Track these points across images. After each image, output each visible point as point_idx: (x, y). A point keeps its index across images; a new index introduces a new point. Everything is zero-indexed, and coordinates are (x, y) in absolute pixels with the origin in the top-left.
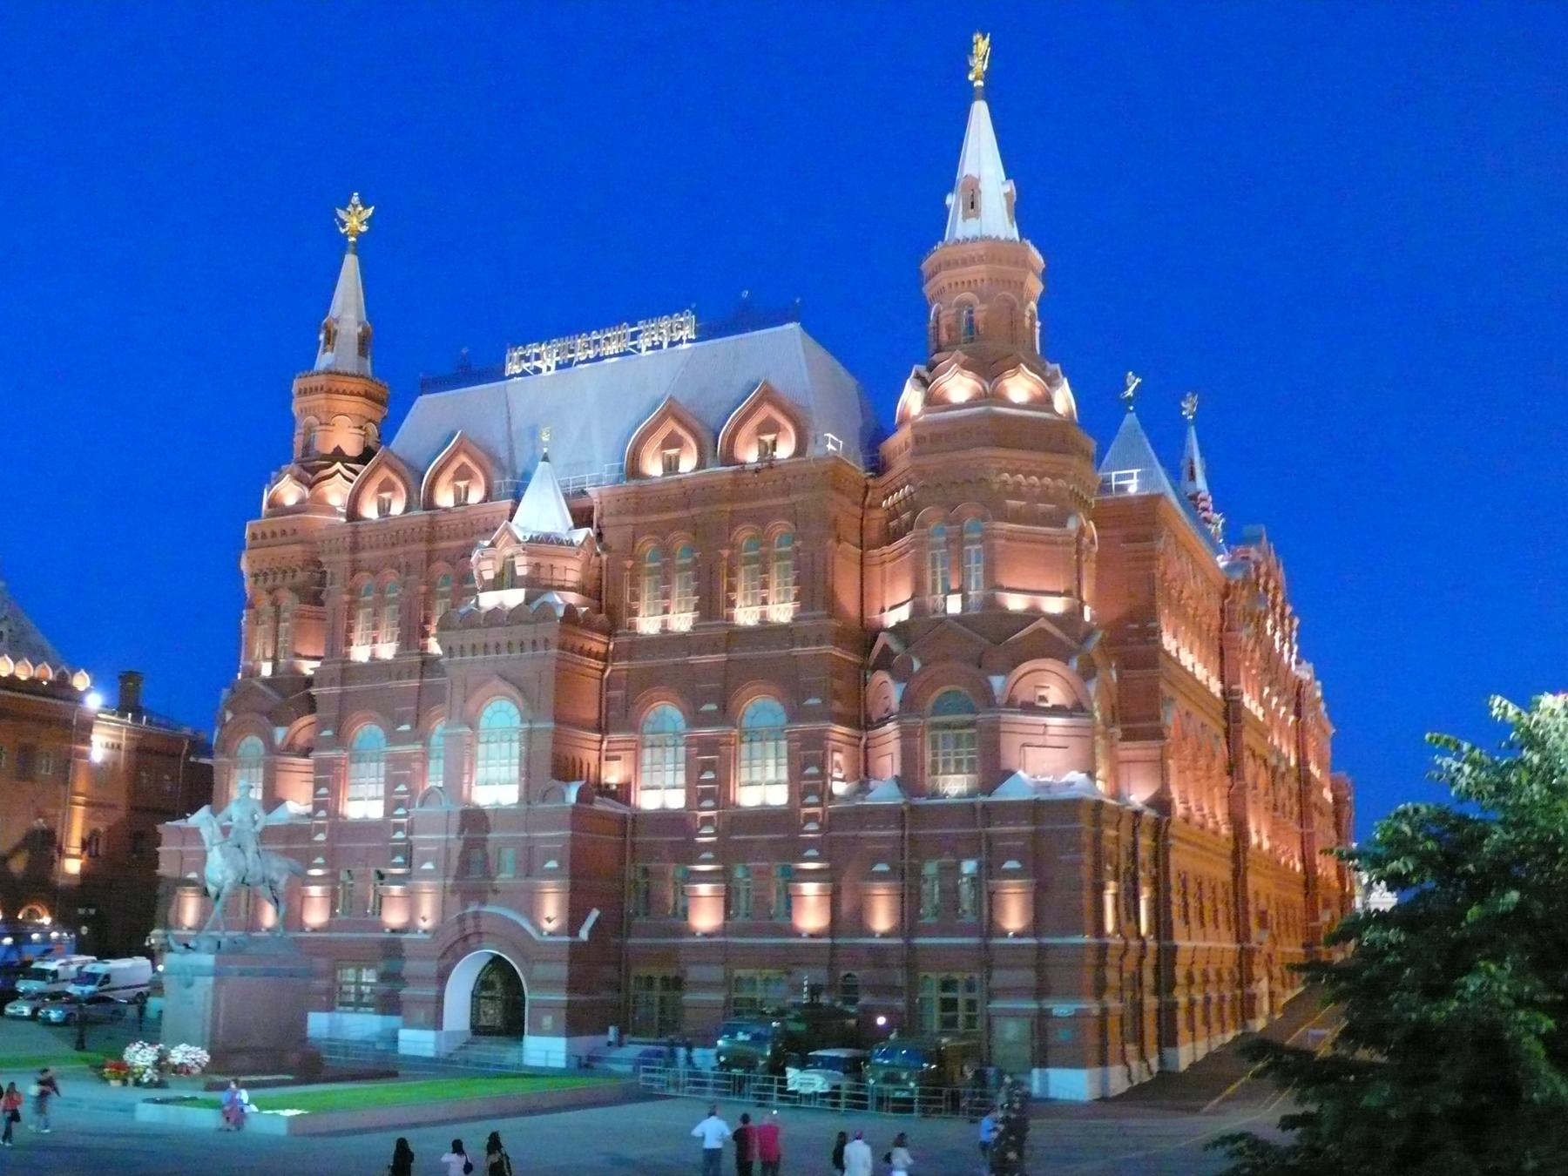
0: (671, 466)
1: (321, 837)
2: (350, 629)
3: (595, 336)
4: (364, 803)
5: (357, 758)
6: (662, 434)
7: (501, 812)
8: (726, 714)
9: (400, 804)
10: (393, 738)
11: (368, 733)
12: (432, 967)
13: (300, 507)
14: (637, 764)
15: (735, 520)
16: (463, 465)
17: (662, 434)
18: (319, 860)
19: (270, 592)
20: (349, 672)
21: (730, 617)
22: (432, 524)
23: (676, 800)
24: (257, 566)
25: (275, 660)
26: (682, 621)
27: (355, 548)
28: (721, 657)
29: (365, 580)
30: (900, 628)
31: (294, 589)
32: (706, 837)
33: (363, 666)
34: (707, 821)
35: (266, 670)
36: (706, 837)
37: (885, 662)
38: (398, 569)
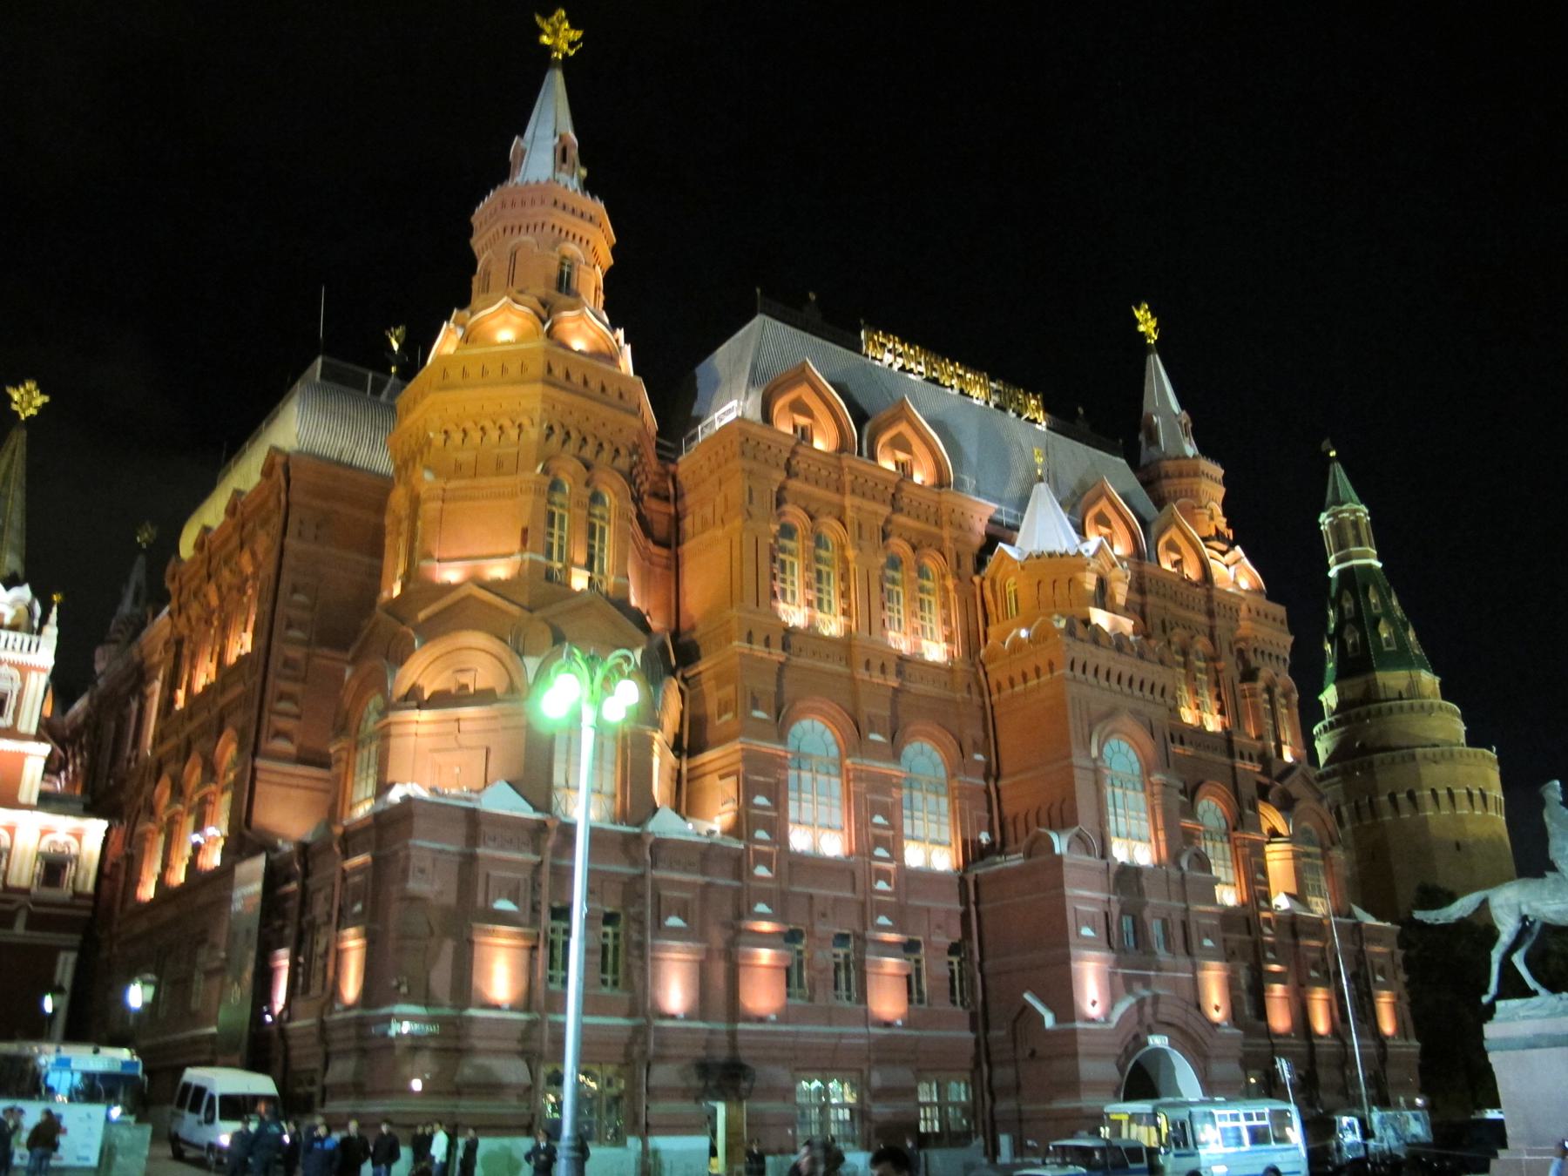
4: (819, 832)
28: (1189, 751)
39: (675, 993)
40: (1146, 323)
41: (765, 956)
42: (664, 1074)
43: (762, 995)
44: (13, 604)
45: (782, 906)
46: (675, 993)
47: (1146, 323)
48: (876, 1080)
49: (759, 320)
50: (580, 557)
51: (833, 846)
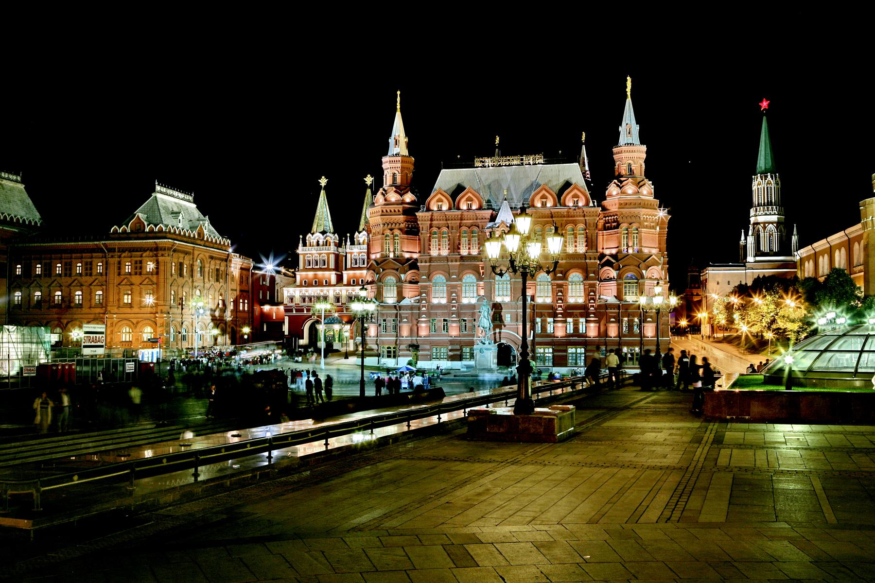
0: (544, 205)
4: (439, 298)
5: (436, 285)
6: (541, 194)
7: (506, 304)
8: (565, 277)
9: (453, 299)
10: (449, 279)
15: (567, 223)
17: (541, 194)
19: (391, 230)
20: (431, 259)
22: (462, 215)
23: (549, 301)
25: (394, 252)
27: (431, 220)
29: (435, 229)
30: (611, 255)
31: (401, 229)
32: (560, 310)
33: (435, 258)
34: (561, 306)
35: (392, 255)
36: (560, 310)
37: (609, 264)
38: (448, 227)
41: (423, 325)
42: (402, 347)
43: (423, 332)
45: (429, 315)
46: (405, 331)
48: (450, 348)
49: (443, 171)
50: (392, 250)
51: (444, 301)
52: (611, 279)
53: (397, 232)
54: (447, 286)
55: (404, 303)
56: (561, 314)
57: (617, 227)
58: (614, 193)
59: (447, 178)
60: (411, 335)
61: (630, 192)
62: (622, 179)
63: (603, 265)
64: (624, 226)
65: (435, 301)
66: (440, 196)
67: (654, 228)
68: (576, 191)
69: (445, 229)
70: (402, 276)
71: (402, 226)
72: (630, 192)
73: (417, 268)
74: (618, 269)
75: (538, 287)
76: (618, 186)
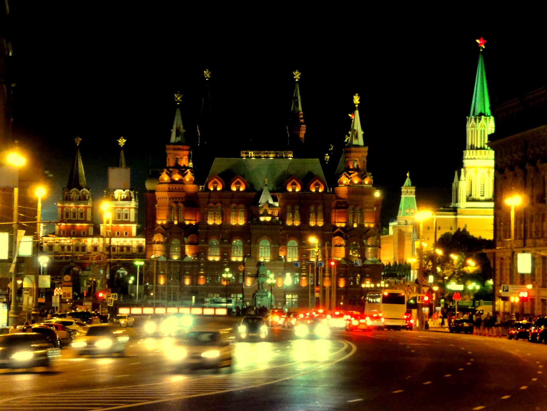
1: (202, 264)
2: (207, 216)
3: (266, 152)
4: (214, 257)
10: (222, 241)
11: (214, 242)
12: (251, 294)
13: (181, 182)
14: (286, 252)
16: (238, 181)
18: (202, 270)
19: (176, 203)
20: (209, 227)
21: (309, 224)
24: (170, 196)
25: (178, 220)
26: (297, 223)
30: (341, 228)
35: (176, 223)
39: (187, 282)
40: (356, 100)
41: (202, 277)
44: (125, 194)
45: (206, 269)
46: (187, 282)
47: (356, 100)
50: (176, 218)
51: (217, 259)
52: (341, 246)
53: (181, 205)
54: (221, 248)
55: (186, 260)
56: (304, 270)
57: (346, 207)
58: (344, 182)
59: (220, 164)
60: (192, 283)
61: (356, 182)
62: (350, 172)
63: (335, 235)
64: (351, 207)
65: (211, 259)
66: (215, 179)
67: (372, 208)
68: (317, 181)
69: (219, 205)
70: (185, 239)
71: (184, 200)
72: (356, 182)
73: (197, 234)
74: (346, 239)
75: (288, 250)
76: (347, 177)
